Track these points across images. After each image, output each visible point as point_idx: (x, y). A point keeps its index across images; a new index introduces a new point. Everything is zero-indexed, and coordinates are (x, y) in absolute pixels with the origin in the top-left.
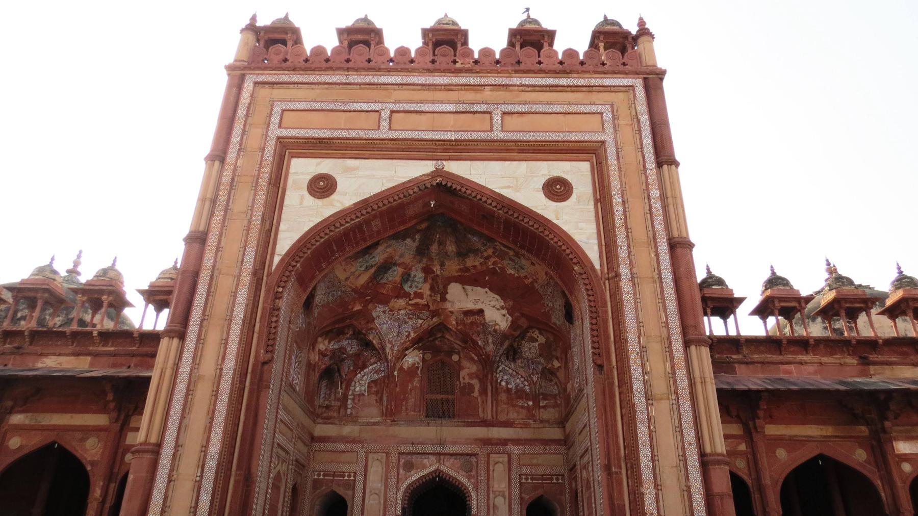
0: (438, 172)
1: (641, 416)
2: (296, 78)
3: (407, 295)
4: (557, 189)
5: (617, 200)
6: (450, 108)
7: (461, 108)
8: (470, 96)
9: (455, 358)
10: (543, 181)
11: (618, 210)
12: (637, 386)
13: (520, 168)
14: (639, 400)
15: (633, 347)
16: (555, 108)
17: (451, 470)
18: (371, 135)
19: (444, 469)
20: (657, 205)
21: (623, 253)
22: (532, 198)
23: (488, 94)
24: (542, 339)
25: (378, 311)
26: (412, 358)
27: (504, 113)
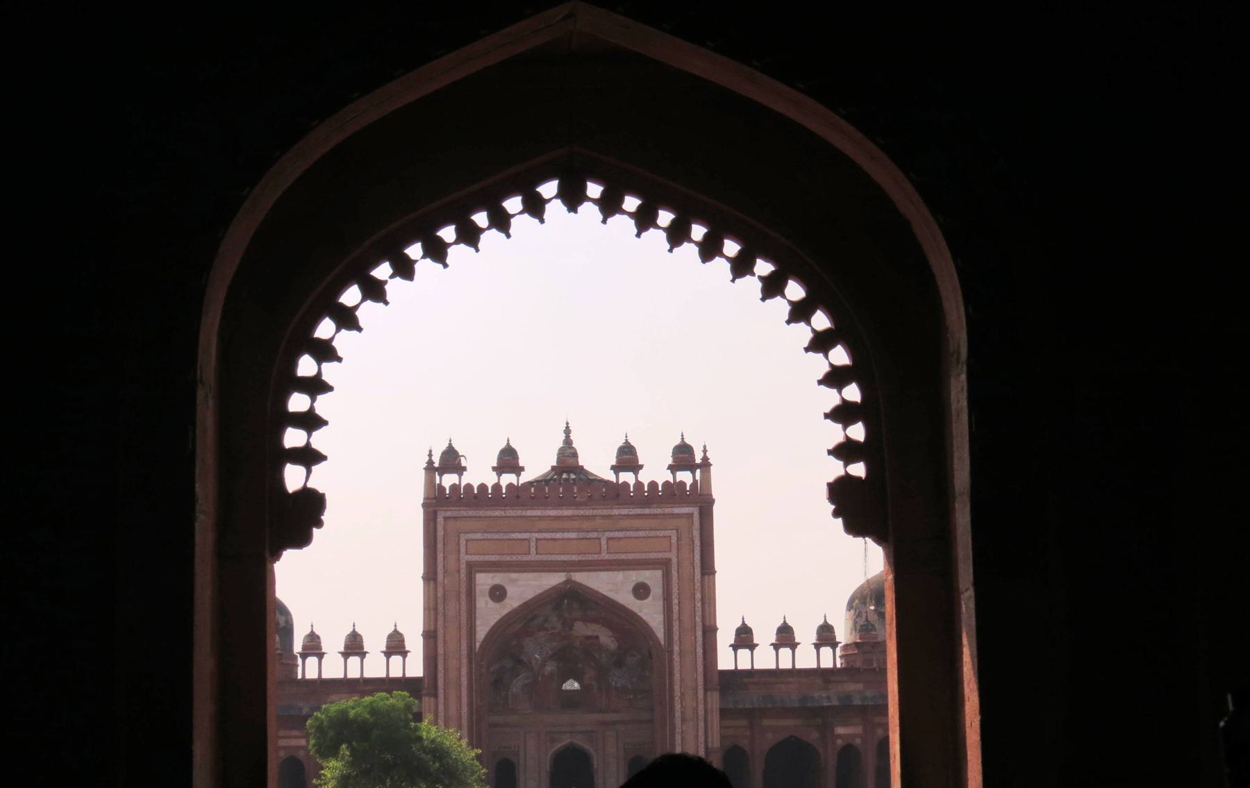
0: (568, 581)
1: (678, 730)
2: (471, 513)
3: (546, 629)
4: (641, 591)
5: (675, 601)
6: (573, 535)
7: (582, 535)
8: (586, 525)
9: (580, 665)
10: (631, 586)
11: (676, 608)
12: (678, 714)
13: (619, 576)
14: (678, 722)
15: (677, 693)
16: (641, 534)
17: (580, 742)
18: (525, 558)
19: (575, 741)
20: (699, 605)
21: (676, 638)
22: (625, 598)
23: (598, 521)
24: (639, 657)
25: (528, 643)
26: (550, 667)
27: (609, 539)
